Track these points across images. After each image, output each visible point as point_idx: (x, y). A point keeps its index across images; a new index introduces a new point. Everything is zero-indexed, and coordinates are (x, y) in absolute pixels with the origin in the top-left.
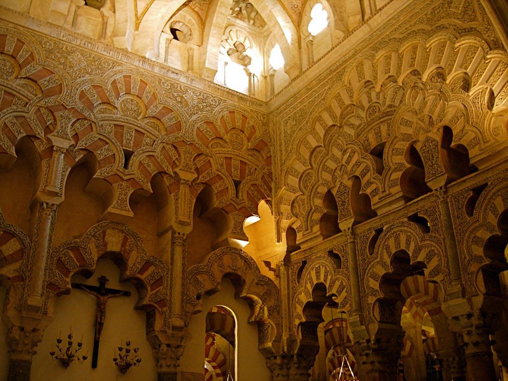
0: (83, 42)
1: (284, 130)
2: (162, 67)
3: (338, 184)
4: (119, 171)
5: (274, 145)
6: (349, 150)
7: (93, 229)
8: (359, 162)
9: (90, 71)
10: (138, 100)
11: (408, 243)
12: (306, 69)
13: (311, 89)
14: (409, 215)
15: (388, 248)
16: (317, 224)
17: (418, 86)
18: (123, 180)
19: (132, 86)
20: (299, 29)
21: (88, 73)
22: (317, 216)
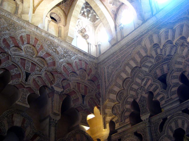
0: (6, 14)
1: (107, 71)
2: (46, 33)
3: (139, 96)
4: (22, 82)
5: (101, 79)
6: (146, 79)
7: (6, 113)
8: (151, 84)
9: (9, 29)
10: (33, 47)
11: (183, 124)
12: (119, 40)
13: (123, 50)
14: (182, 110)
15: (171, 128)
16: (128, 118)
17: (184, 45)
18: (24, 87)
19: (30, 40)
20: (116, 22)
21: (8, 30)
22: (127, 114)
